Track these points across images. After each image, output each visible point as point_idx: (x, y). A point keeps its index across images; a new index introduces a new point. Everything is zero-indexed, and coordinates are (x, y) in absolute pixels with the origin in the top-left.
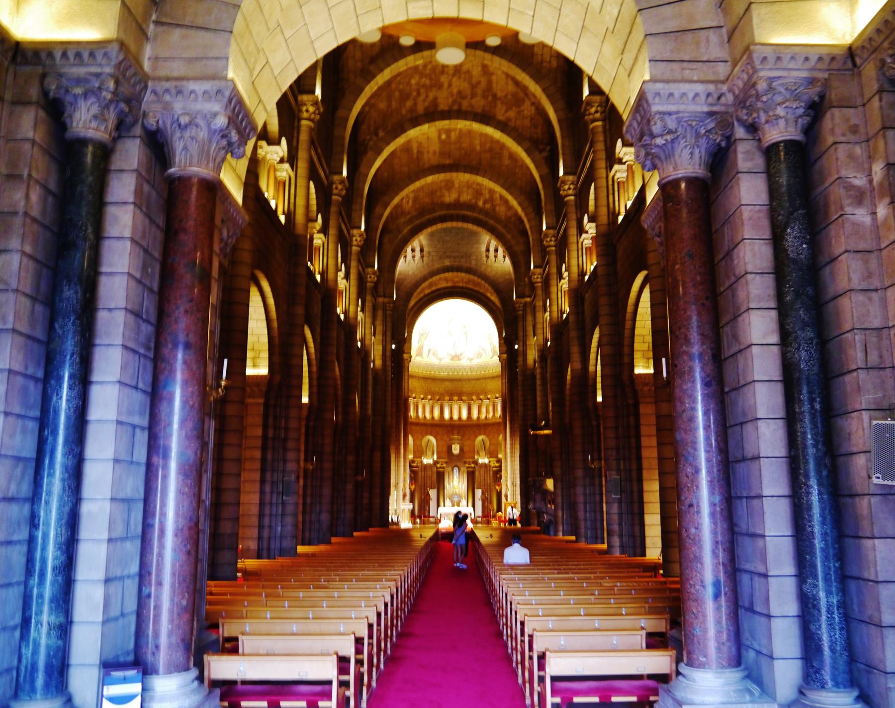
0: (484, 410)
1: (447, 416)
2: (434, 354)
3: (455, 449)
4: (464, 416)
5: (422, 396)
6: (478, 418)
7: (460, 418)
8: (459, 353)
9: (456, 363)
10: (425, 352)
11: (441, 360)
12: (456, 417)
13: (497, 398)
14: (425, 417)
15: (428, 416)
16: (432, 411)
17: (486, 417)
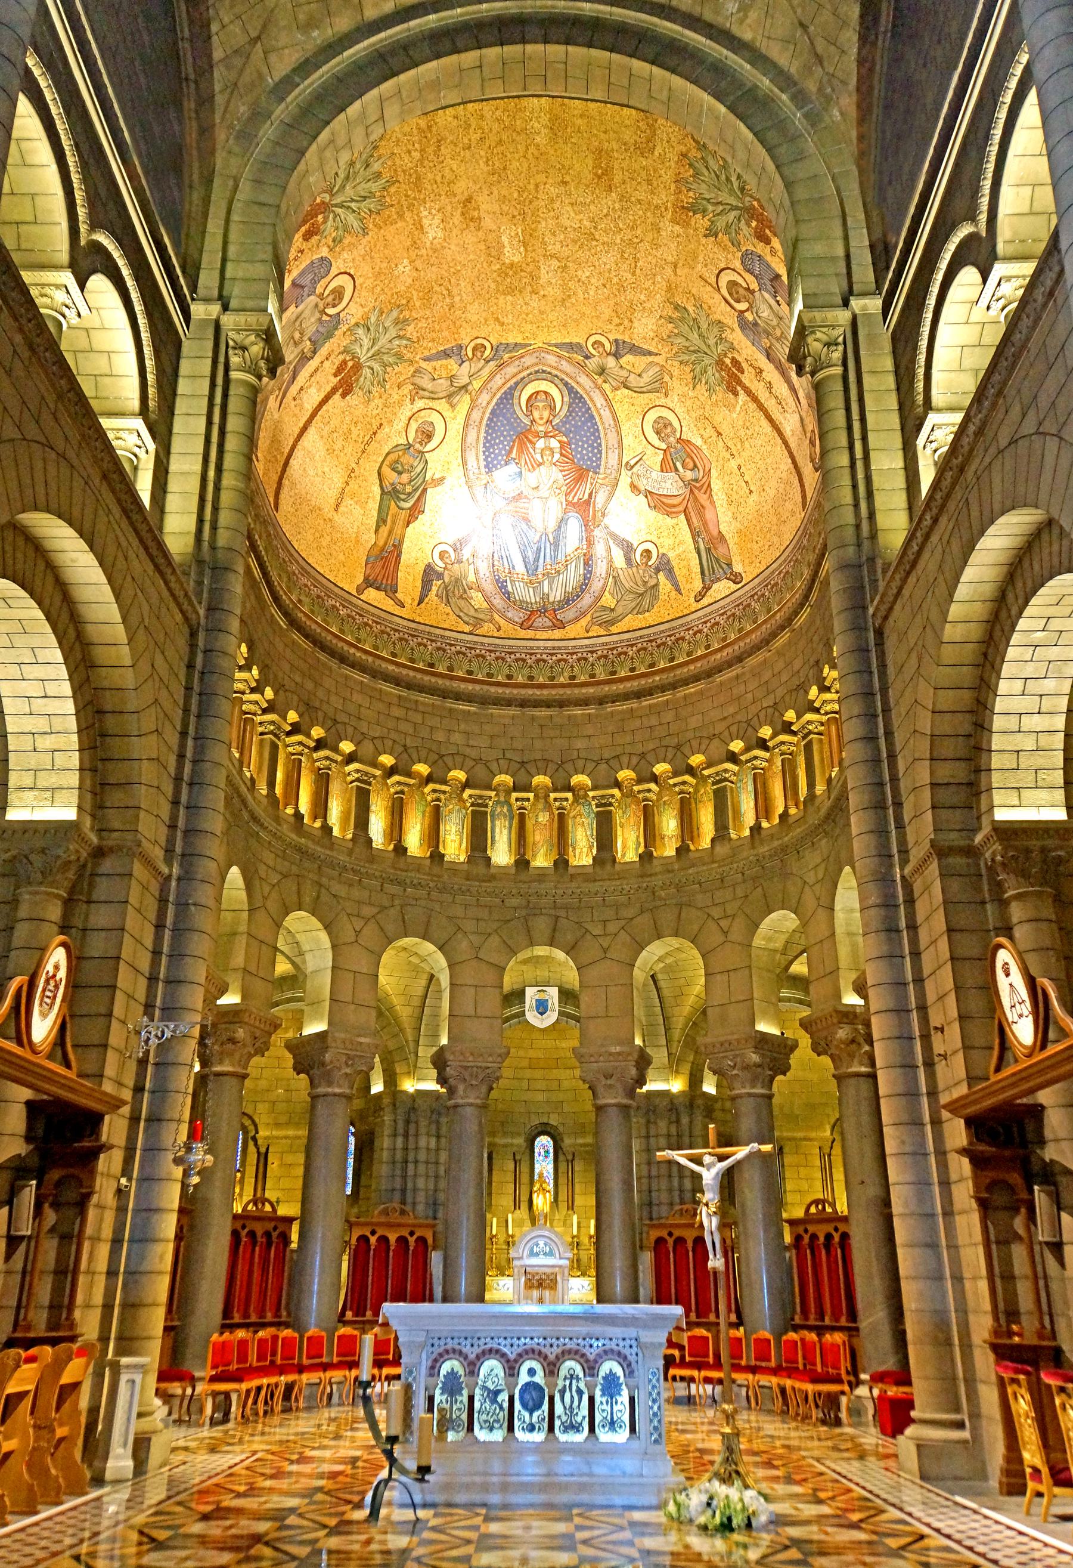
0: (669, 825)
1: (501, 855)
2: (446, 596)
3: (542, 1007)
4: (582, 854)
5: (387, 760)
6: (646, 857)
7: (562, 863)
8: (556, 595)
9: (544, 638)
10: (408, 581)
11: (478, 622)
12: (542, 860)
13: (733, 758)
14: (400, 850)
15: (414, 841)
16: (433, 835)
17: (682, 851)
